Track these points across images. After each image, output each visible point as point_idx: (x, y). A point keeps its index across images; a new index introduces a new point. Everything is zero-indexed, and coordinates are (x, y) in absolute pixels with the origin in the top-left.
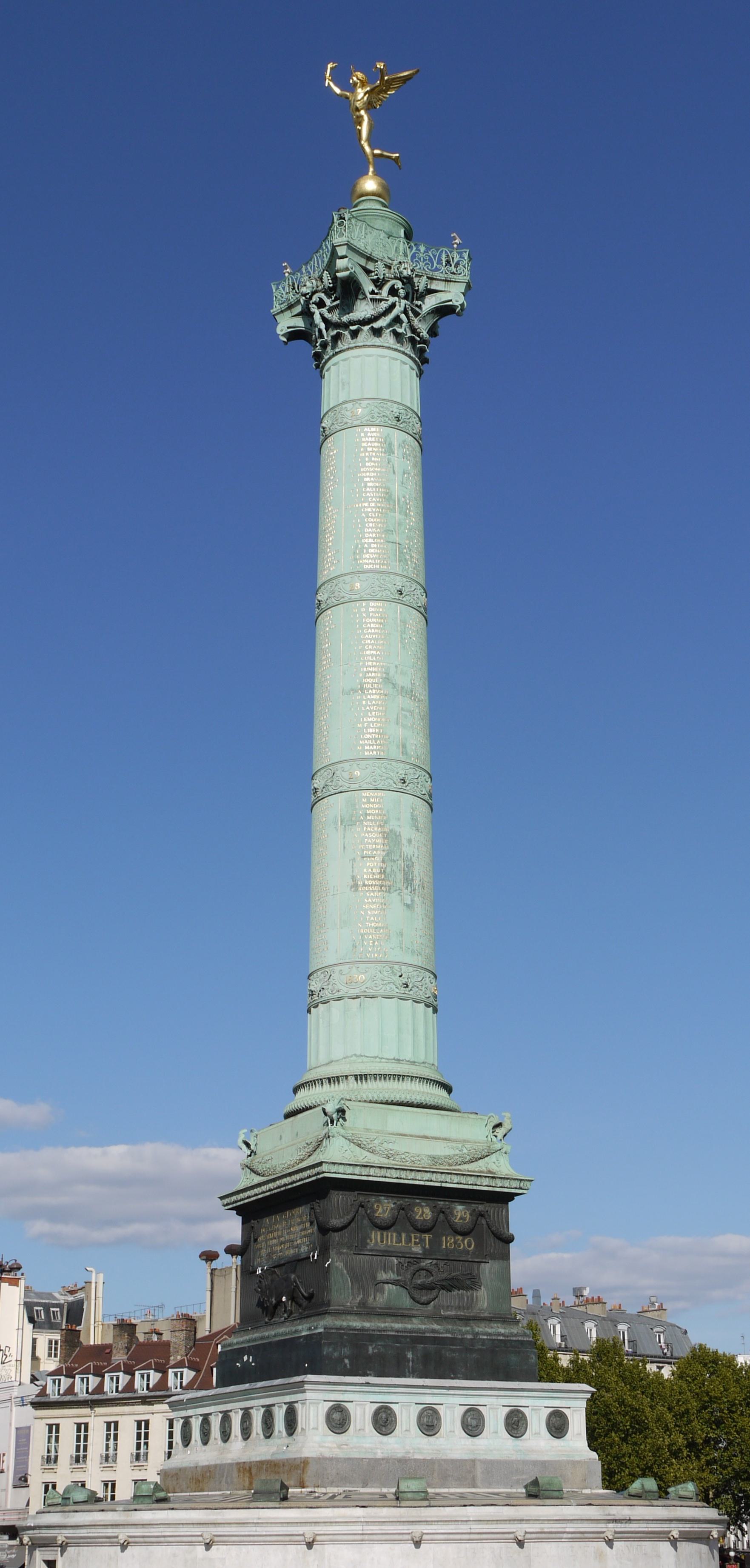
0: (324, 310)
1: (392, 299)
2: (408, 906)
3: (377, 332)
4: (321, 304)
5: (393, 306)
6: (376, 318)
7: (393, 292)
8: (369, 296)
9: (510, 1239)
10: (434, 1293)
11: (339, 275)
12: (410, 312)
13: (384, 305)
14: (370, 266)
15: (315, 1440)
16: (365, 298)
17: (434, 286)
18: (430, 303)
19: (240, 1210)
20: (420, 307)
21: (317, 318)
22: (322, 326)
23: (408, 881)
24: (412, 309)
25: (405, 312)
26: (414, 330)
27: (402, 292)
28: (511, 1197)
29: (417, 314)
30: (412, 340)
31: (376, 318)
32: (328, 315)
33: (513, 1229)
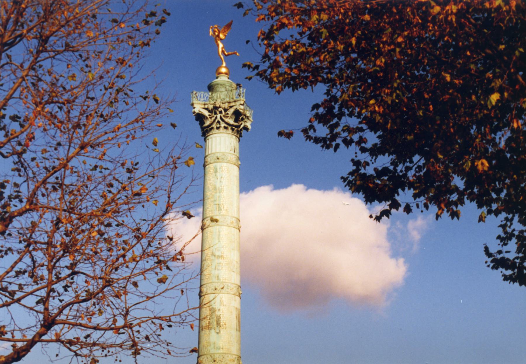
1: (215, 116)
2: (218, 333)
5: (216, 118)
6: (212, 124)
8: (208, 117)
12: (223, 118)
13: (213, 118)
14: (206, 107)
16: (207, 118)
17: (231, 105)
18: (231, 111)
20: (228, 114)
23: (218, 324)
24: (224, 116)
25: (221, 118)
26: (226, 123)
27: (218, 112)
29: (228, 117)
30: (225, 128)
31: (212, 124)
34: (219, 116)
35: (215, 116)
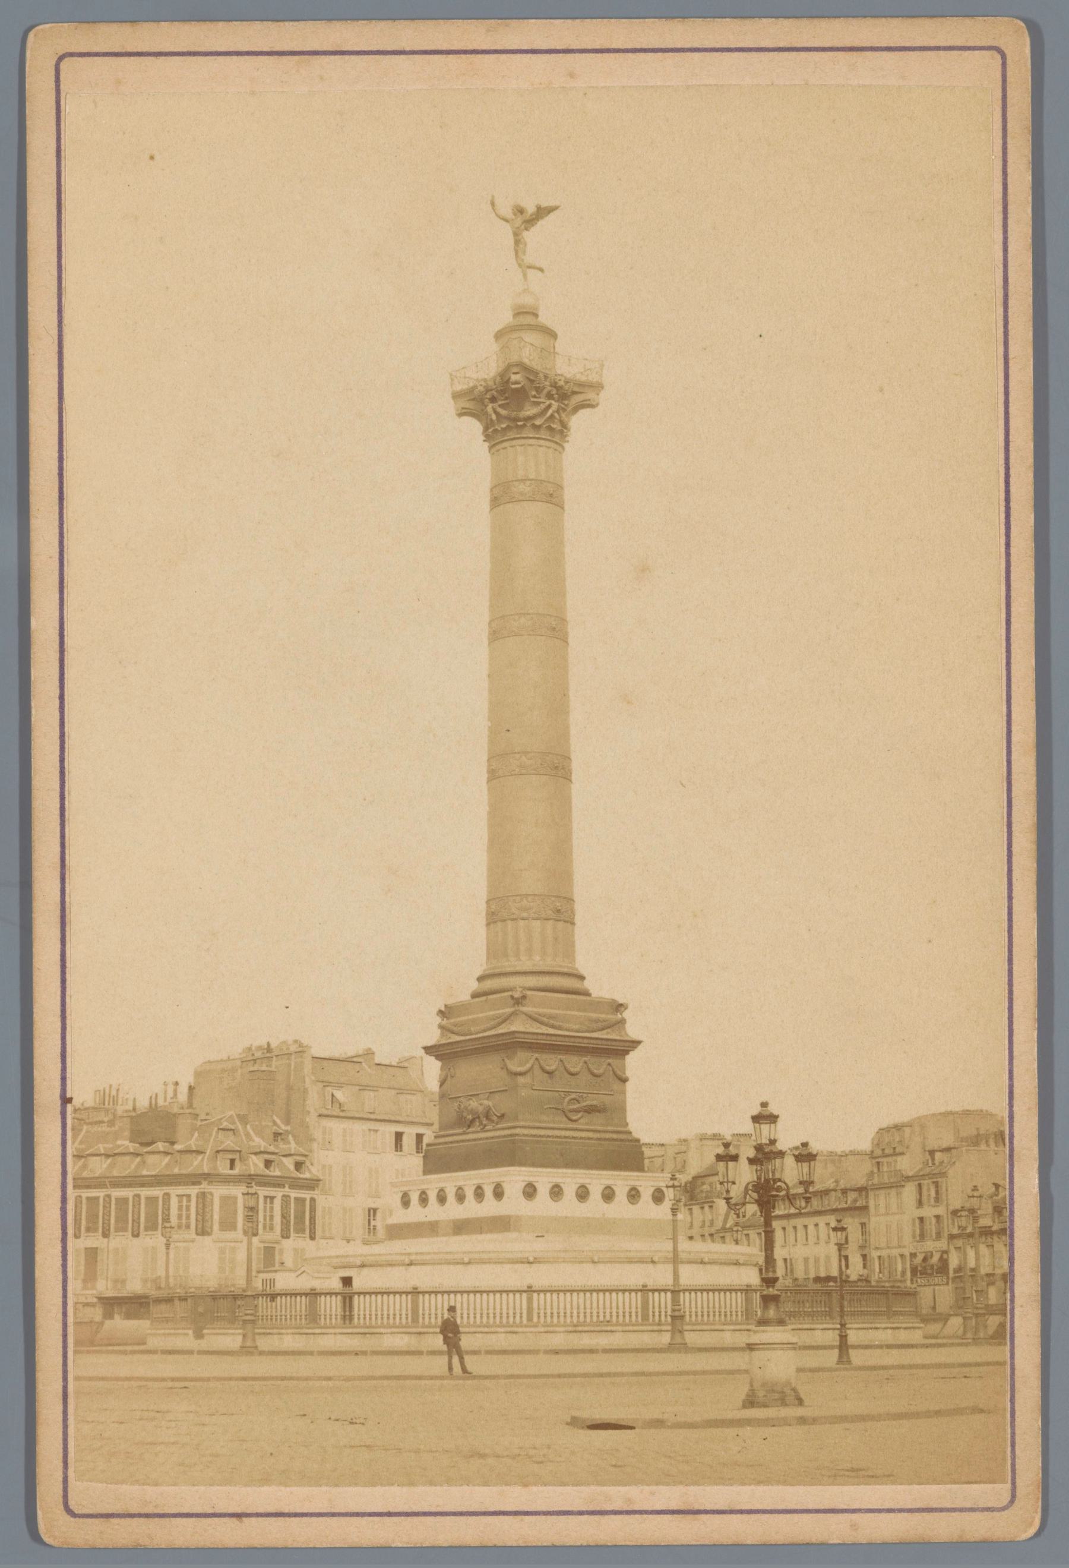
0: (496, 405)
3: (537, 428)
4: (493, 400)
5: (550, 406)
7: (550, 396)
9: (624, 1080)
10: (580, 1115)
11: (513, 386)
13: (543, 406)
15: (514, 1204)
19: (438, 1057)
21: (489, 408)
22: (494, 417)
28: (627, 1052)
32: (500, 410)
33: (628, 1073)
34: (555, 405)
35: (548, 402)
